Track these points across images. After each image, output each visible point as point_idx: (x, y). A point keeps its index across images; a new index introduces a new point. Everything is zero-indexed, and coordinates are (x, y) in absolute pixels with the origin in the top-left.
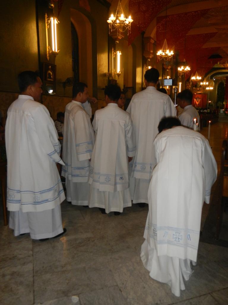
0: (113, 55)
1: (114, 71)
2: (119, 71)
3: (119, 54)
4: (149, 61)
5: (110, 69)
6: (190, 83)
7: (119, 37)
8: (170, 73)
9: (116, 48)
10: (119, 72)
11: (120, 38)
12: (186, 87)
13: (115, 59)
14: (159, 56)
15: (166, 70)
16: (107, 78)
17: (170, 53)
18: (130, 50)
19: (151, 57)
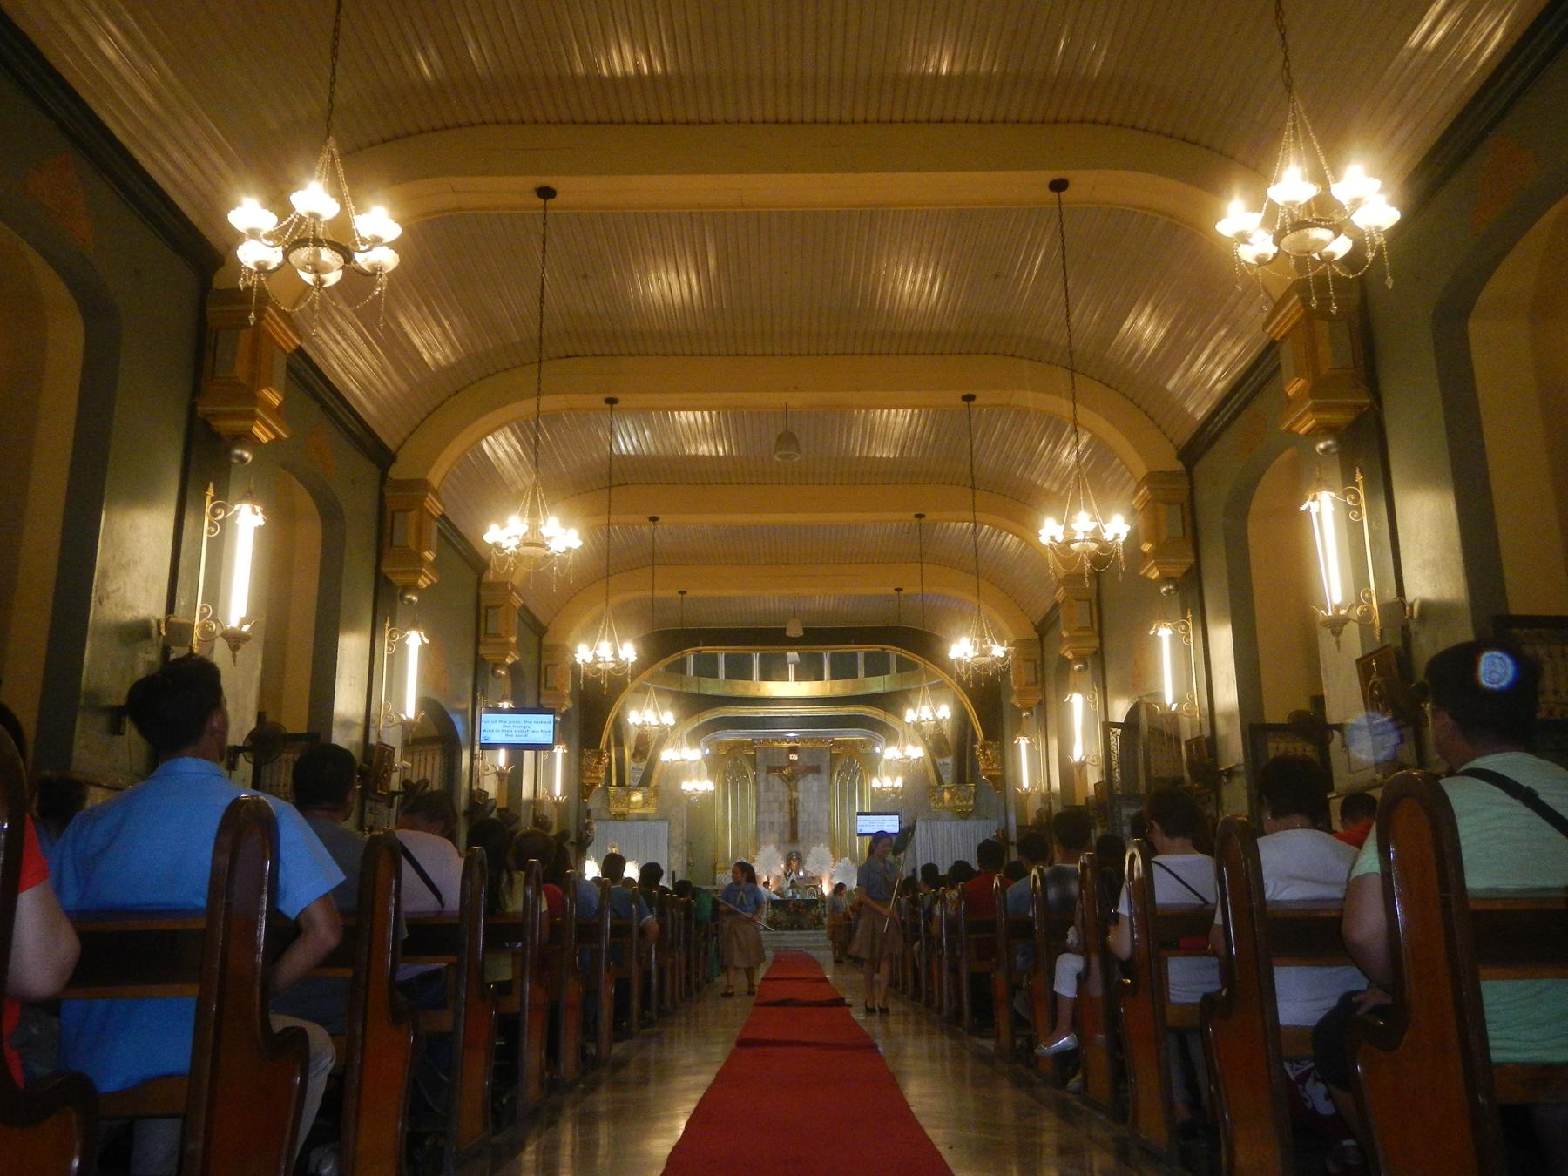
0: (211, 524)
1: (202, 616)
2: (243, 614)
3: (248, 520)
4: (410, 601)
5: (181, 601)
6: (600, 755)
7: (256, 430)
8: (507, 687)
9: (234, 491)
10: (243, 622)
11: (265, 440)
12: (581, 773)
13: (219, 546)
14: (497, 546)
15: (493, 671)
16: (153, 656)
17: (563, 536)
18: (311, 532)
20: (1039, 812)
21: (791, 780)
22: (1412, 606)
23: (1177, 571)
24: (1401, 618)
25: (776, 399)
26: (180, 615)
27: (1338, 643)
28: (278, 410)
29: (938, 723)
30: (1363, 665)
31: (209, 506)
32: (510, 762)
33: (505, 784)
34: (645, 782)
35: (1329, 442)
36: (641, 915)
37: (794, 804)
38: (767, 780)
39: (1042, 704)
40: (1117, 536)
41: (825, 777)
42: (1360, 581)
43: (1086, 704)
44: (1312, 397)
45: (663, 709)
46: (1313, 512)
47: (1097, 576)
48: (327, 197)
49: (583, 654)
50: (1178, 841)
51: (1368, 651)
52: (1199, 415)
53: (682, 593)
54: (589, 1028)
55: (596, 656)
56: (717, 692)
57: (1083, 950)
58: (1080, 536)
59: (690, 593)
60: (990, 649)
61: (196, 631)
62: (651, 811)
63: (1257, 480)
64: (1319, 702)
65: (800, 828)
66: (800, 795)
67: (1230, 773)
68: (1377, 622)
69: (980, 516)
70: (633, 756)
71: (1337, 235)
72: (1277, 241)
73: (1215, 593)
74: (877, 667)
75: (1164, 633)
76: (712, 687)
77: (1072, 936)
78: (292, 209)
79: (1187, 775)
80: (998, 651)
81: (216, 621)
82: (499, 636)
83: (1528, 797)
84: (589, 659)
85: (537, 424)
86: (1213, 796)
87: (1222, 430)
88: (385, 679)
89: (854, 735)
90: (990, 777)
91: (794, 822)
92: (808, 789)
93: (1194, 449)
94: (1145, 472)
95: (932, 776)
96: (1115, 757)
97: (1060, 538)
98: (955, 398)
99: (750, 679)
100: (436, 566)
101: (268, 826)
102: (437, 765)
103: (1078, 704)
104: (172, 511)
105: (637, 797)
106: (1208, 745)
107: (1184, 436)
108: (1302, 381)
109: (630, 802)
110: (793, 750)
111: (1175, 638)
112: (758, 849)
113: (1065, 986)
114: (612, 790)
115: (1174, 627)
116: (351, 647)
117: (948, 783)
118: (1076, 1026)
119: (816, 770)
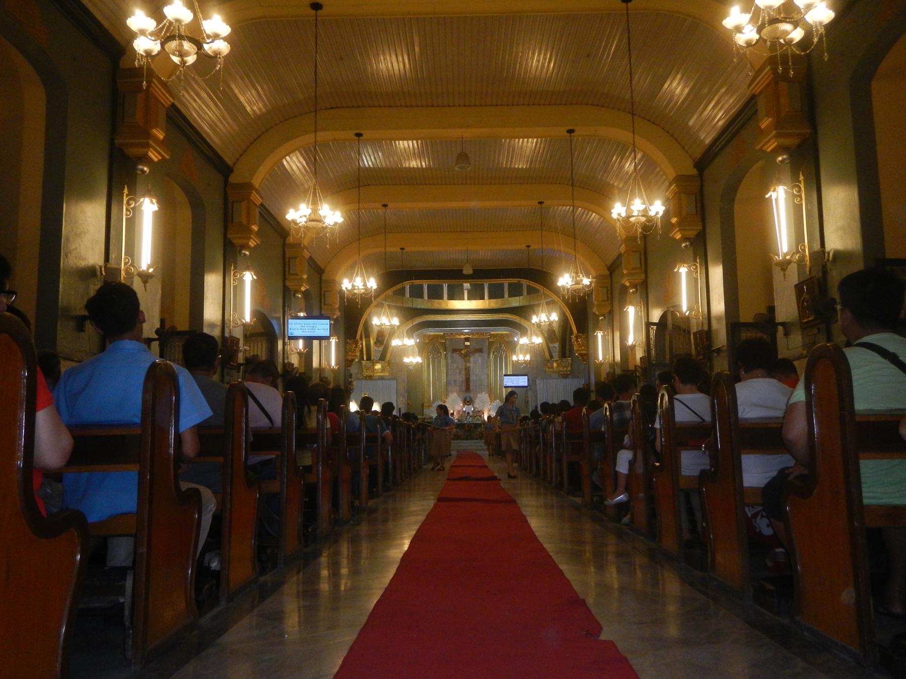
0: (127, 210)
1: (126, 264)
3: (149, 207)
4: (245, 255)
5: (113, 255)
6: (356, 343)
7: (150, 154)
8: (303, 304)
10: (149, 267)
11: (156, 160)
12: (346, 352)
14: (294, 222)
15: (294, 295)
17: (332, 216)
18: (185, 215)
19: (252, 244)
20: (608, 374)
21: (466, 356)
22: (829, 253)
23: (692, 234)
24: (822, 261)
25: (455, 133)
26: (112, 264)
27: (785, 275)
28: (163, 140)
29: (551, 323)
30: (799, 288)
31: (125, 199)
32: (305, 347)
33: (303, 359)
34: (382, 358)
35: (785, 157)
36: (383, 430)
37: (468, 370)
38: (452, 357)
39: (611, 313)
40: (657, 213)
41: (485, 355)
42: (799, 239)
43: (636, 312)
44: (775, 129)
45: (392, 316)
46: (773, 198)
47: (645, 237)
48: (185, 9)
49: (346, 285)
50: (688, 386)
51: (802, 279)
52: (708, 141)
53: (402, 249)
54: (355, 491)
55: (353, 286)
56: (423, 307)
57: (633, 447)
58: (635, 213)
59: (407, 249)
60: (582, 280)
61: (122, 272)
62: (386, 374)
63: (740, 181)
64: (772, 309)
65: (471, 384)
66: (471, 365)
67: (719, 351)
68: (808, 263)
69: (576, 203)
70: (375, 343)
71: (795, 28)
72: (759, 31)
73: (714, 246)
74: (515, 291)
75: (683, 270)
76: (420, 304)
77: (627, 439)
78: (164, 17)
79: (693, 352)
80: (586, 281)
81: (134, 266)
82: (296, 274)
83: (893, 358)
84: (350, 287)
85: (315, 149)
86: (708, 364)
87: (722, 149)
88: (233, 299)
89: (502, 331)
90: (580, 354)
91: (468, 380)
92: (475, 362)
93: (704, 162)
94: (674, 175)
95: (547, 354)
96: (652, 342)
97: (624, 215)
98: (562, 131)
99: (441, 298)
100: (258, 234)
101: (173, 378)
102: (264, 349)
103: (631, 312)
104: (105, 203)
105: (378, 366)
106: (706, 335)
107: (698, 153)
108: (770, 119)
109: (374, 370)
110: (467, 340)
111: (689, 274)
112: (447, 395)
113: (622, 467)
114: (364, 363)
115: (689, 267)
116: (212, 282)
117: (556, 356)
118: (627, 489)
119: (480, 351)
